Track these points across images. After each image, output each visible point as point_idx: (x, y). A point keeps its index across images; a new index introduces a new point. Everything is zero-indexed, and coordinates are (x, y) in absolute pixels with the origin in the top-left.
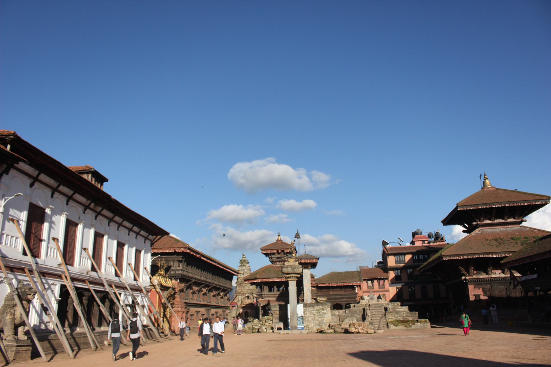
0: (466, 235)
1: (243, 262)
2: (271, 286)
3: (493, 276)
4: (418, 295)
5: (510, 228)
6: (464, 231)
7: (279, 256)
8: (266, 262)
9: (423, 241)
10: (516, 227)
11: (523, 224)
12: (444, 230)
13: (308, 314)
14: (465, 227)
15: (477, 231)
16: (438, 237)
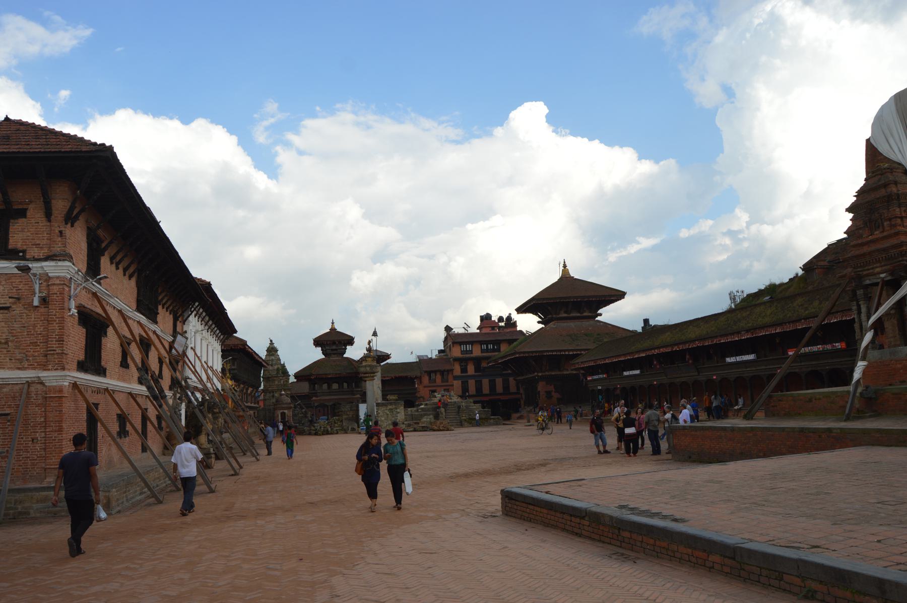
0: (541, 326)
1: (272, 350)
2: (329, 380)
3: (565, 373)
4: (486, 389)
5: (586, 323)
6: (539, 322)
7: (334, 347)
8: (317, 354)
9: (493, 328)
10: (591, 322)
11: (599, 318)
12: (516, 317)
13: (381, 414)
14: (540, 317)
15: (551, 325)
16: (510, 323)
